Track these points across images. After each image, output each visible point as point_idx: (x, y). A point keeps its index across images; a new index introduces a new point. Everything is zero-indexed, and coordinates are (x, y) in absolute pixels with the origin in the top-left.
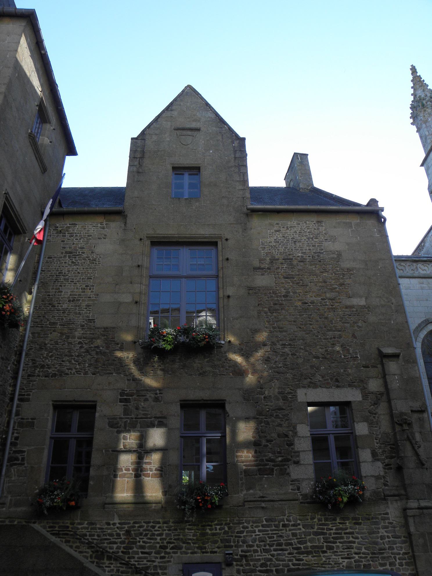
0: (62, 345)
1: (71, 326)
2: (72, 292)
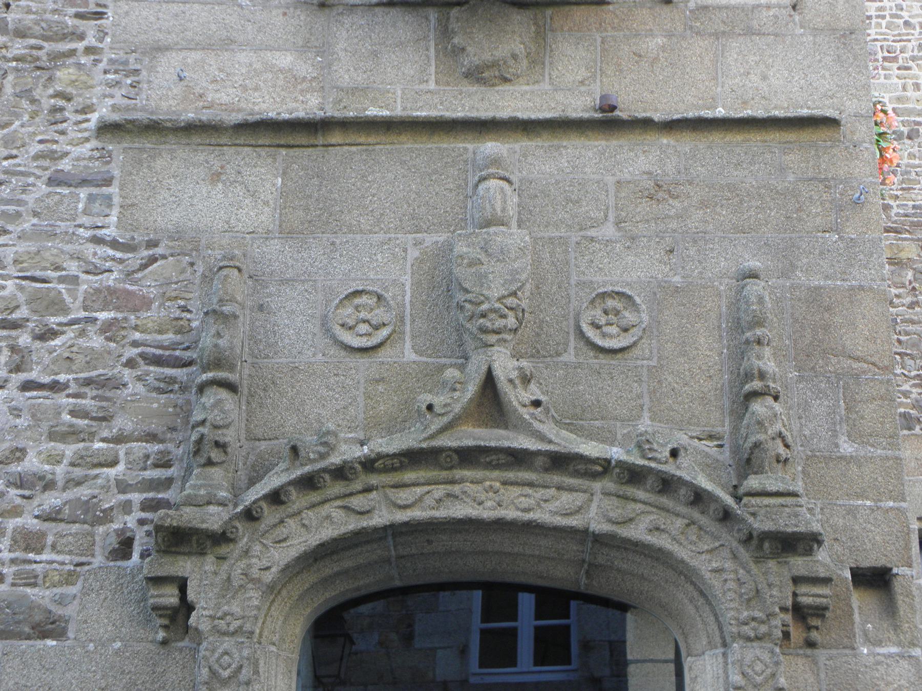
0: (912, 306)
2: (899, 99)
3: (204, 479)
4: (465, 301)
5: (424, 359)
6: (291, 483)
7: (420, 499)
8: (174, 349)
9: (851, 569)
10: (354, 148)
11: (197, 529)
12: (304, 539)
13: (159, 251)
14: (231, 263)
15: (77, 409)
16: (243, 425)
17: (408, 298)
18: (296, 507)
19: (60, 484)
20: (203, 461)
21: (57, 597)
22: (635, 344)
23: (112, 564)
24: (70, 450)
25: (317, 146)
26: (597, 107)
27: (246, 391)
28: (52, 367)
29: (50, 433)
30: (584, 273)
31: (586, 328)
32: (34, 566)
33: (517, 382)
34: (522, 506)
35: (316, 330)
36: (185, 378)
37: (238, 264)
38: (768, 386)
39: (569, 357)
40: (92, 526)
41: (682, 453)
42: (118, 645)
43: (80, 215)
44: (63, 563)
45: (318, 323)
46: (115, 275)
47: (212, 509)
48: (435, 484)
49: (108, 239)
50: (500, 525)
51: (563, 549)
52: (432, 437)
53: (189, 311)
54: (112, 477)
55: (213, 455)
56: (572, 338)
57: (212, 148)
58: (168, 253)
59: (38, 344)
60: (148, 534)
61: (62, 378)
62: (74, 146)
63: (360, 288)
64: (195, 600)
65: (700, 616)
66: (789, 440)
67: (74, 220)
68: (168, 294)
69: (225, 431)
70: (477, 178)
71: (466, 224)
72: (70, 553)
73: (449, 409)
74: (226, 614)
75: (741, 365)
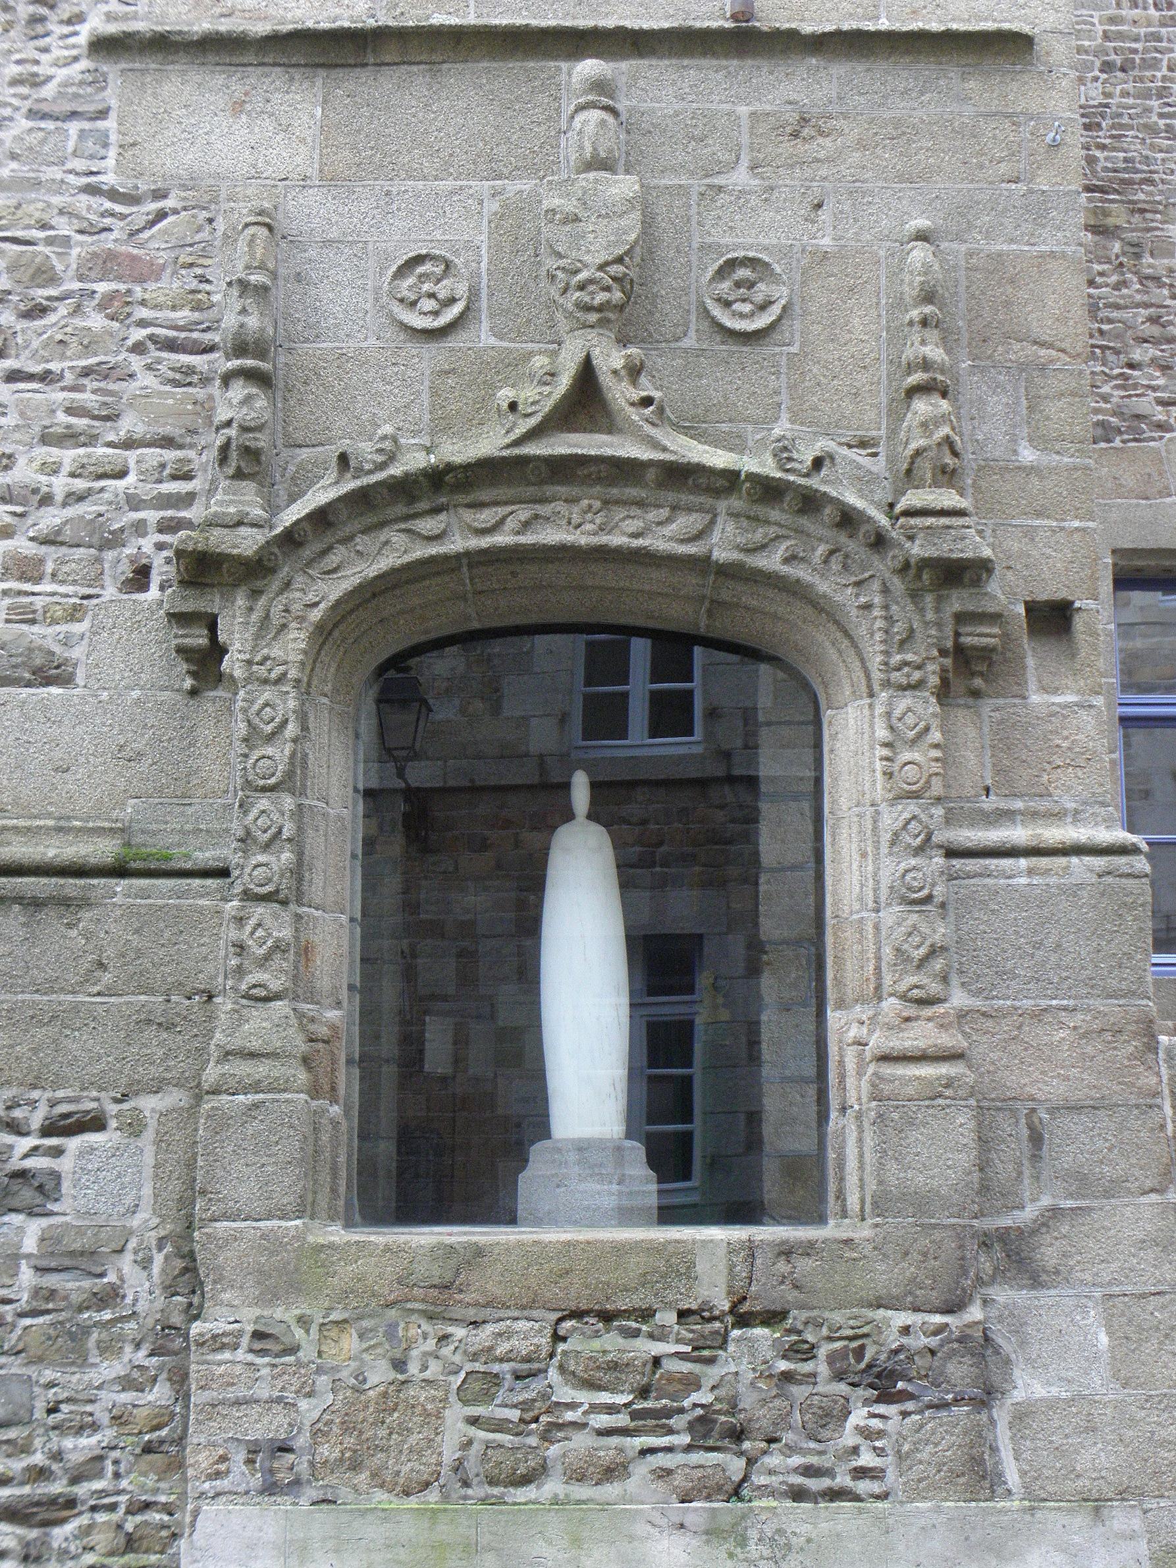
0: (1117, 287)
1: (1142, 196)
2: (1112, 20)
3: (234, 494)
4: (558, 268)
5: (505, 344)
6: (340, 499)
7: (502, 521)
8: (191, 331)
9: (1026, 603)
10: (415, 68)
11: (229, 555)
12: (359, 569)
13: (169, 203)
14: (260, 219)
15: (75, 405)
16: (280, 428)
17: (484, 265)
18: (348, 530)
19: (59, 498)
20: (231, 471)
21: (61, 636)
22: (772, 327)
23: (126, 597)
24: (69, 456)
25: (366, 65)
26: (728, 15)
27: (281, 385)
28: (41, 352)
29: (42, 436)
30: (709, 233)
31: (710, 304)
32: (31, 599)
33: (623, 373)
34: (631, 530)
35: (368, 306)
36: (206, 367)
37: (268, 220)
38: (935, 379)
39: (689, 342)
40: (101, 549)
41: (827, 462)
42: (135, 694)
43: (70, 157)
44: (67, 596)
45: (370, 297)
46: (115, 235)
47: (244, 531)
48: (521, 502)
49: (105, 187)
50: (602, 554)
51: (679, 582)
52: (517, 443)
53: (208, 281)
54: (120, 491)
55: (243, 464)
56: (693, 318)
57: (234, 69)
58: (179, 205)
59: (25, 324)
60: (168, 561)
61: (54, 366)
62: (60, 67)
63: (424, 252)
64: (228, 642)
65: (844, 661)
66: (959, 445)
67: (63, 164)
68: (181, 260)
69: (258, 435)
70: (572, 107)
71: (559, 169)
72: (75, 582)
73: (537, 407)
74: (266, 658)
75: (902, 352)
